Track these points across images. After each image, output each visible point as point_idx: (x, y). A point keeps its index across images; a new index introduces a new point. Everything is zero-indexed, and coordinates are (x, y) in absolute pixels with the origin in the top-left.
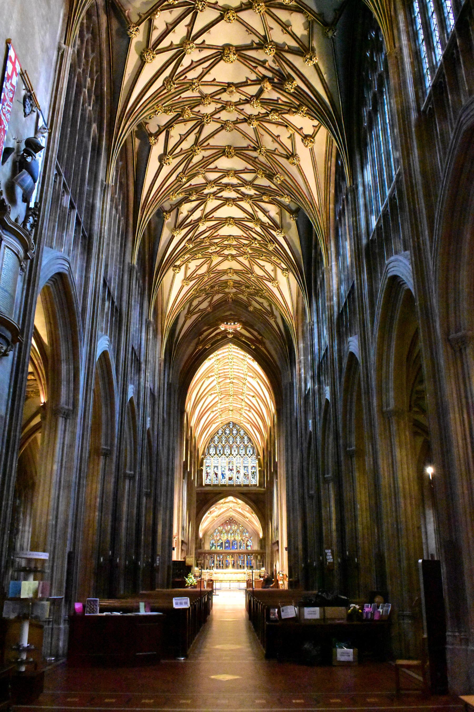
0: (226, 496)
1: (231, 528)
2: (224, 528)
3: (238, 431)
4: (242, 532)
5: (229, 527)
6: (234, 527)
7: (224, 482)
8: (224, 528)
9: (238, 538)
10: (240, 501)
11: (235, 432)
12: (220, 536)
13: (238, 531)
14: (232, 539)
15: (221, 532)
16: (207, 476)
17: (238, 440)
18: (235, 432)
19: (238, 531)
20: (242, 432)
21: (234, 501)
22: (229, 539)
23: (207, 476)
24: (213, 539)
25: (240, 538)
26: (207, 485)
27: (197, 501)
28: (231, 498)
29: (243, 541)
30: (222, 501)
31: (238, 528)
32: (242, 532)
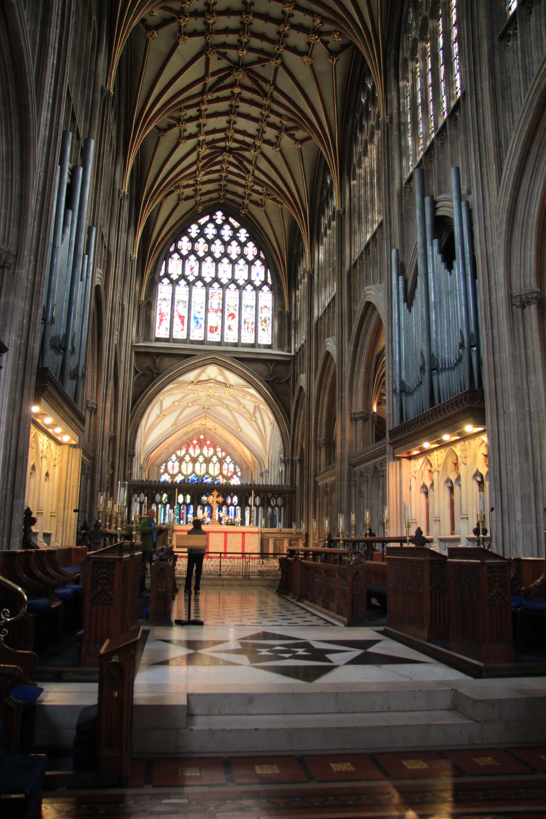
0: (204, 364)
1: (201, 454)
2: (187, 452)
3: (235, 231)
4: (221, 461)
5: (198, 451)
6: (208, 452)
7: (197, 335)
8: (187, 452)
9: (214, 470)
10: (233, 378)
11: (227, 232)
12: (180, 467)
13: (215, 459)
14: (203, 472)
15: (181, 460)
16: (161, 320)
17: (234, 250)
18: (227, 232)
19: (215, 459)
20: (243, 234)
21: (220, 379)
22: (198, 472)
23: (161, 320)
24: (166, 471)
25: (217, 472)
26: (158, 340)
27: (136, 372)
28: (212, 371)
29: (224, 477)
30: (191, 376)
31: (215, 453)
32: (221, 461)
